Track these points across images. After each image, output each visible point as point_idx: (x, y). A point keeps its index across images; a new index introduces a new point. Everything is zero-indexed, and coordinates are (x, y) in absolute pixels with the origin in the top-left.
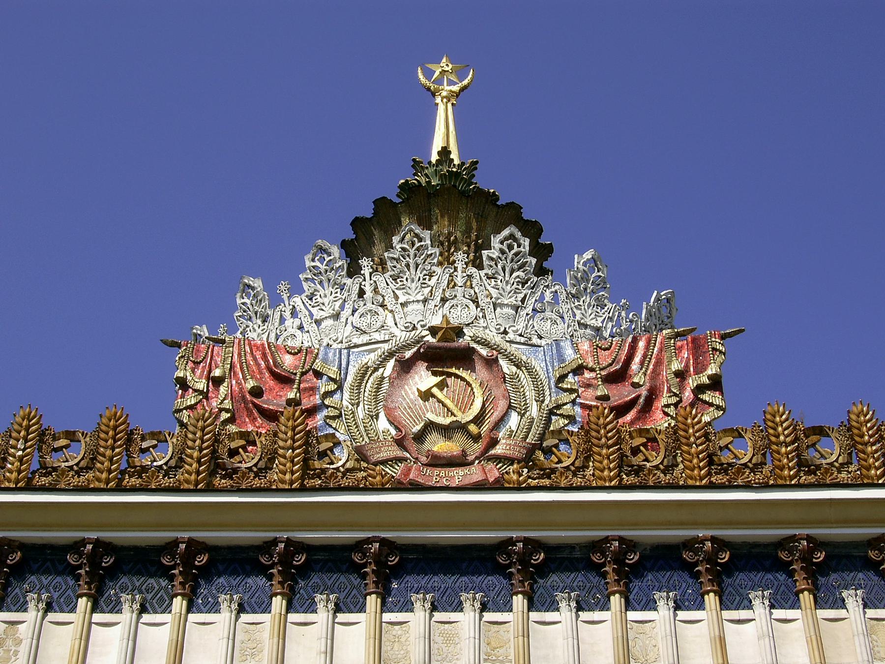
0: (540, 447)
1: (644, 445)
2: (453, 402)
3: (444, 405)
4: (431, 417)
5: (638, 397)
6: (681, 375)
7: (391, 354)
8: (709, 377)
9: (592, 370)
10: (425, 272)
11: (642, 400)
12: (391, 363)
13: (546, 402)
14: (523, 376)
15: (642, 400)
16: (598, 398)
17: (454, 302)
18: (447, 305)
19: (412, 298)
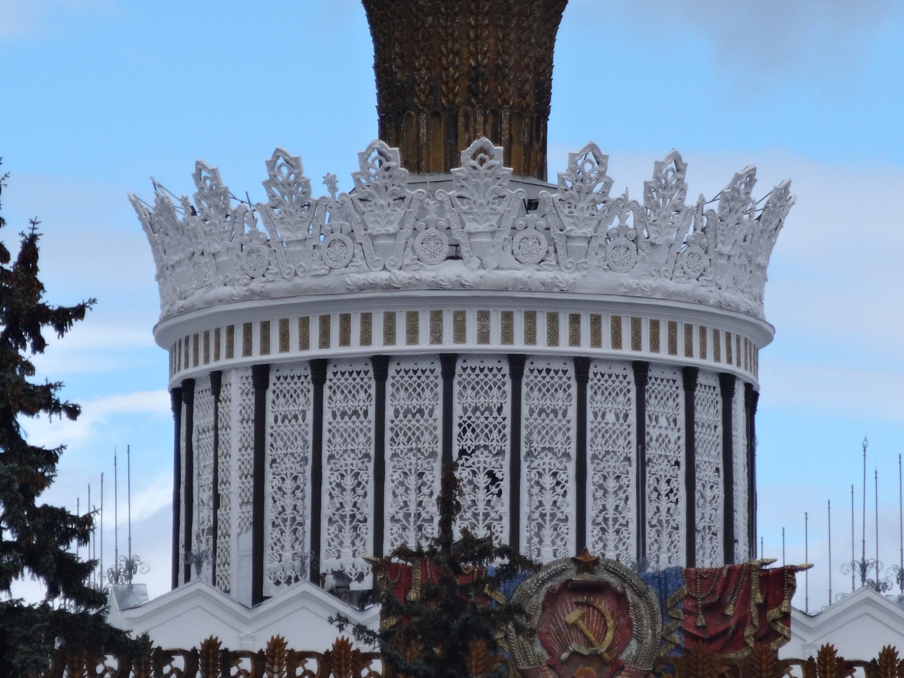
0: (653, 672)
1: (728, 671)
2: (591, 632)
3: (585, 636)
4: (574, 647)
5: (728, 629)
6: (763, 608)
7: (544, 582)
8: (782, 613)
9: (695, 599)
10: (494, 196)
11: (730, 632)
12: (543, 591)
13: (659, 630)
14: (642, 605)
15: (730, 632)
16: (697, 627)
17: (525, 233)
18: (518, 237)
19: (480, 228)
